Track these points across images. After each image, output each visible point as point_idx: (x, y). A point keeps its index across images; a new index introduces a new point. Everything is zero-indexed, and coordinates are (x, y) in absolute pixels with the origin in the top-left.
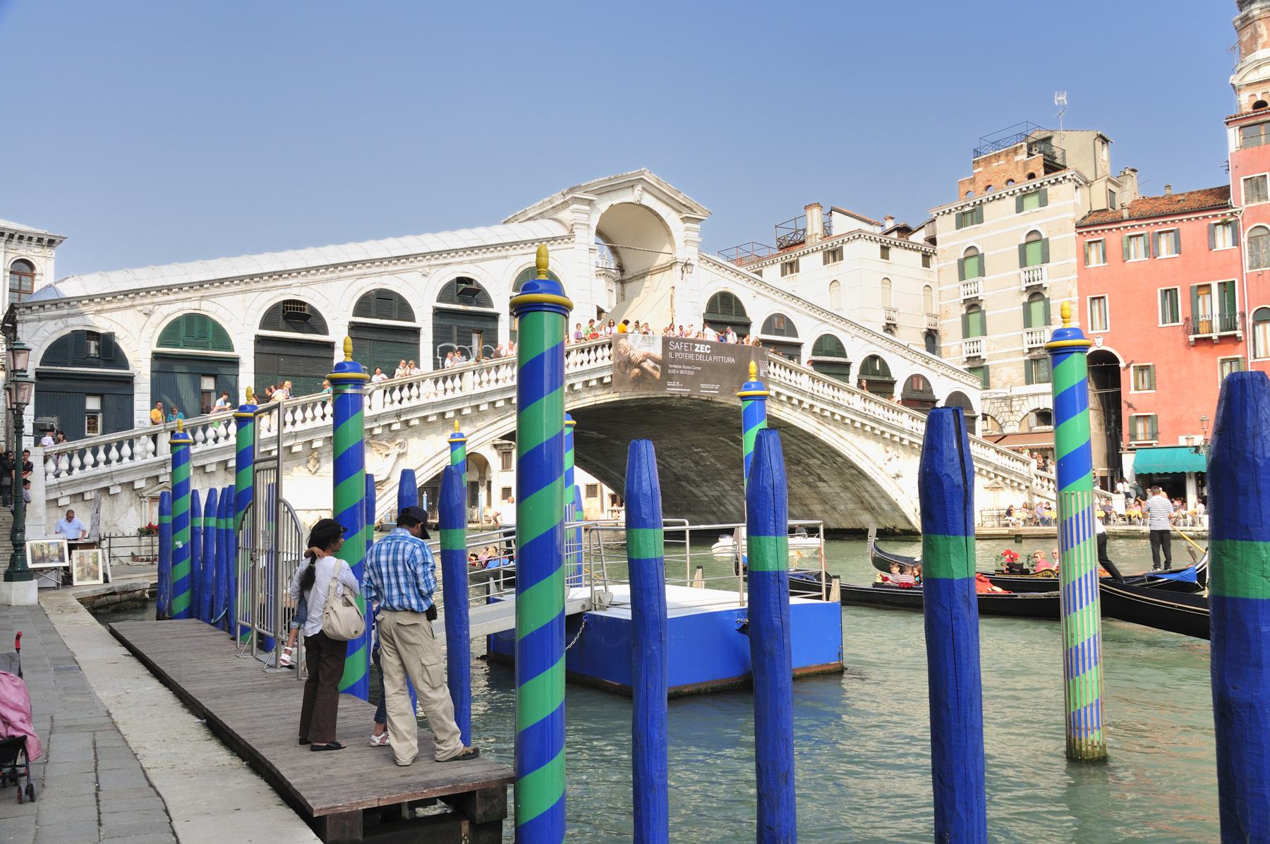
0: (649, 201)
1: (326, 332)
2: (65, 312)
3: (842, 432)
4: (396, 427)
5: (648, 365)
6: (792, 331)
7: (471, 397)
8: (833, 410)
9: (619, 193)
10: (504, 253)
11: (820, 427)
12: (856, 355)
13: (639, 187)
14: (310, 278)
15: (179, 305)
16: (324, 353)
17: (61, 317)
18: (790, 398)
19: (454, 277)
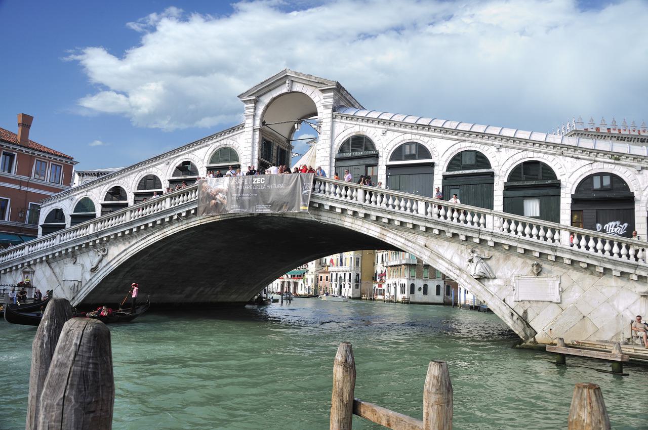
0: (297, 88)
1: (127, 200)
2: (51, 203)
3: (411, 237)
4: (98, 241)
5: (219, 197)
8: (390, 217)
9: (277, 89)
10: (205, 144)
11: (385, 232)
12: (503, 163)
13: (287, 82)
14: (123, 175)
15: (81, 195)
17: (50, 204)
18: (344, 211)
19: (181, 162)
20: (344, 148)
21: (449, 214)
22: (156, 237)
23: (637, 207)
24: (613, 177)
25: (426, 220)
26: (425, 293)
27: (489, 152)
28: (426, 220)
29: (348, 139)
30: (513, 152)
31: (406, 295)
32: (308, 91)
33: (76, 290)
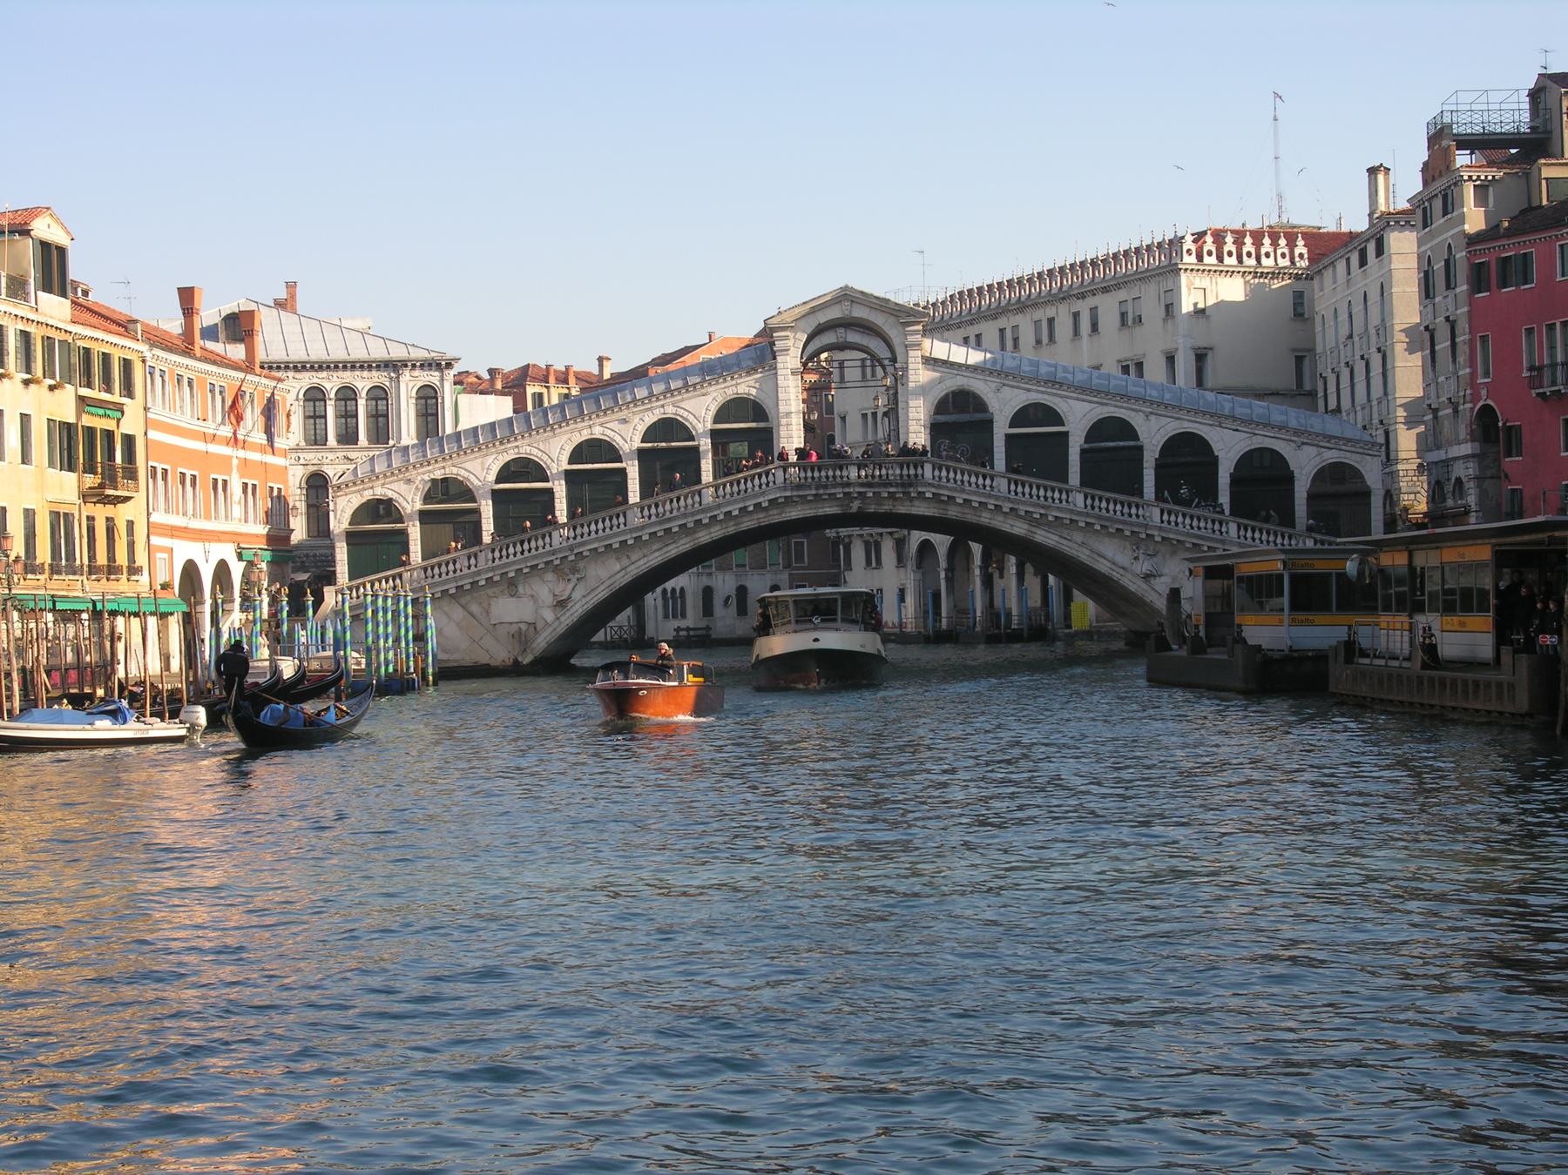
0: (859, 313)
6: (1057, 419)
7: (631, 531)
12: (1153, 433)
16: (546, 498)
20: (942, 406)
21: (1111, 507)
22: (683, 545)
23: (1296, 483)
24: (1272, 451)
25: (1087, 515)
26: (742, 610)
27: (1137, 421)
28: (1087, 515)
29: (947, 395)
30: (1164, 420)
31: (693, 619)
32: (878, 319)
33: (522, 638)
